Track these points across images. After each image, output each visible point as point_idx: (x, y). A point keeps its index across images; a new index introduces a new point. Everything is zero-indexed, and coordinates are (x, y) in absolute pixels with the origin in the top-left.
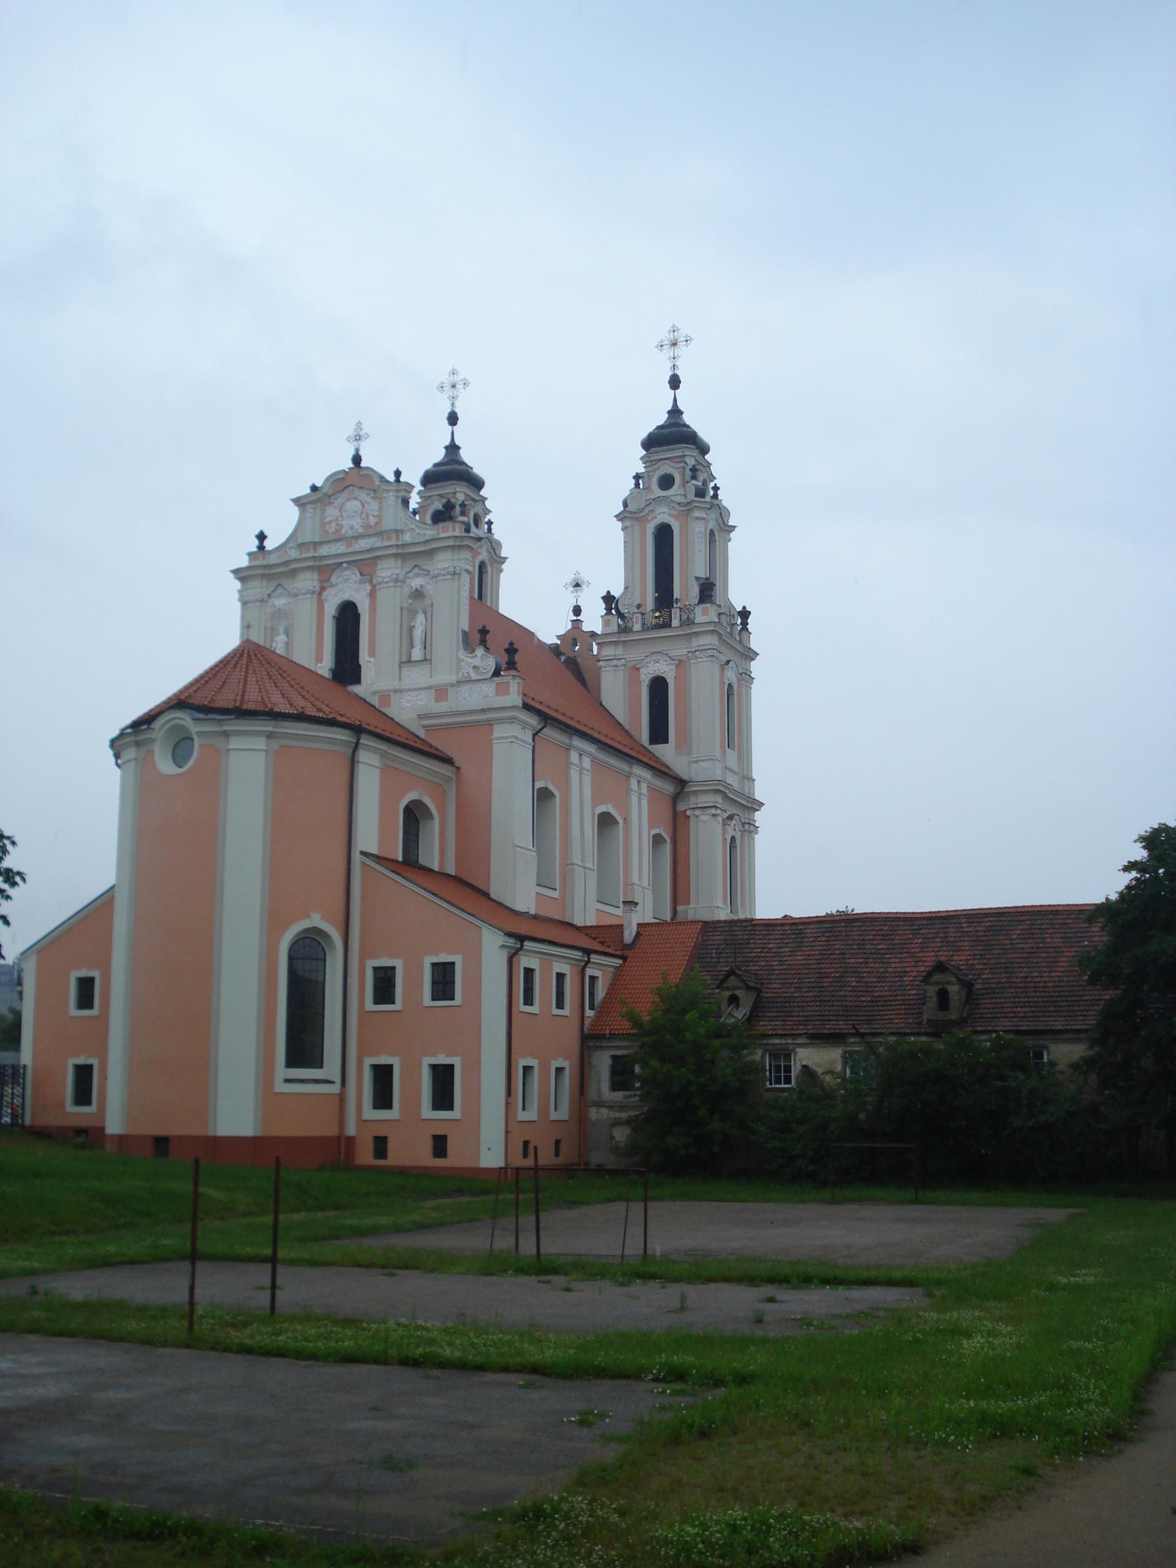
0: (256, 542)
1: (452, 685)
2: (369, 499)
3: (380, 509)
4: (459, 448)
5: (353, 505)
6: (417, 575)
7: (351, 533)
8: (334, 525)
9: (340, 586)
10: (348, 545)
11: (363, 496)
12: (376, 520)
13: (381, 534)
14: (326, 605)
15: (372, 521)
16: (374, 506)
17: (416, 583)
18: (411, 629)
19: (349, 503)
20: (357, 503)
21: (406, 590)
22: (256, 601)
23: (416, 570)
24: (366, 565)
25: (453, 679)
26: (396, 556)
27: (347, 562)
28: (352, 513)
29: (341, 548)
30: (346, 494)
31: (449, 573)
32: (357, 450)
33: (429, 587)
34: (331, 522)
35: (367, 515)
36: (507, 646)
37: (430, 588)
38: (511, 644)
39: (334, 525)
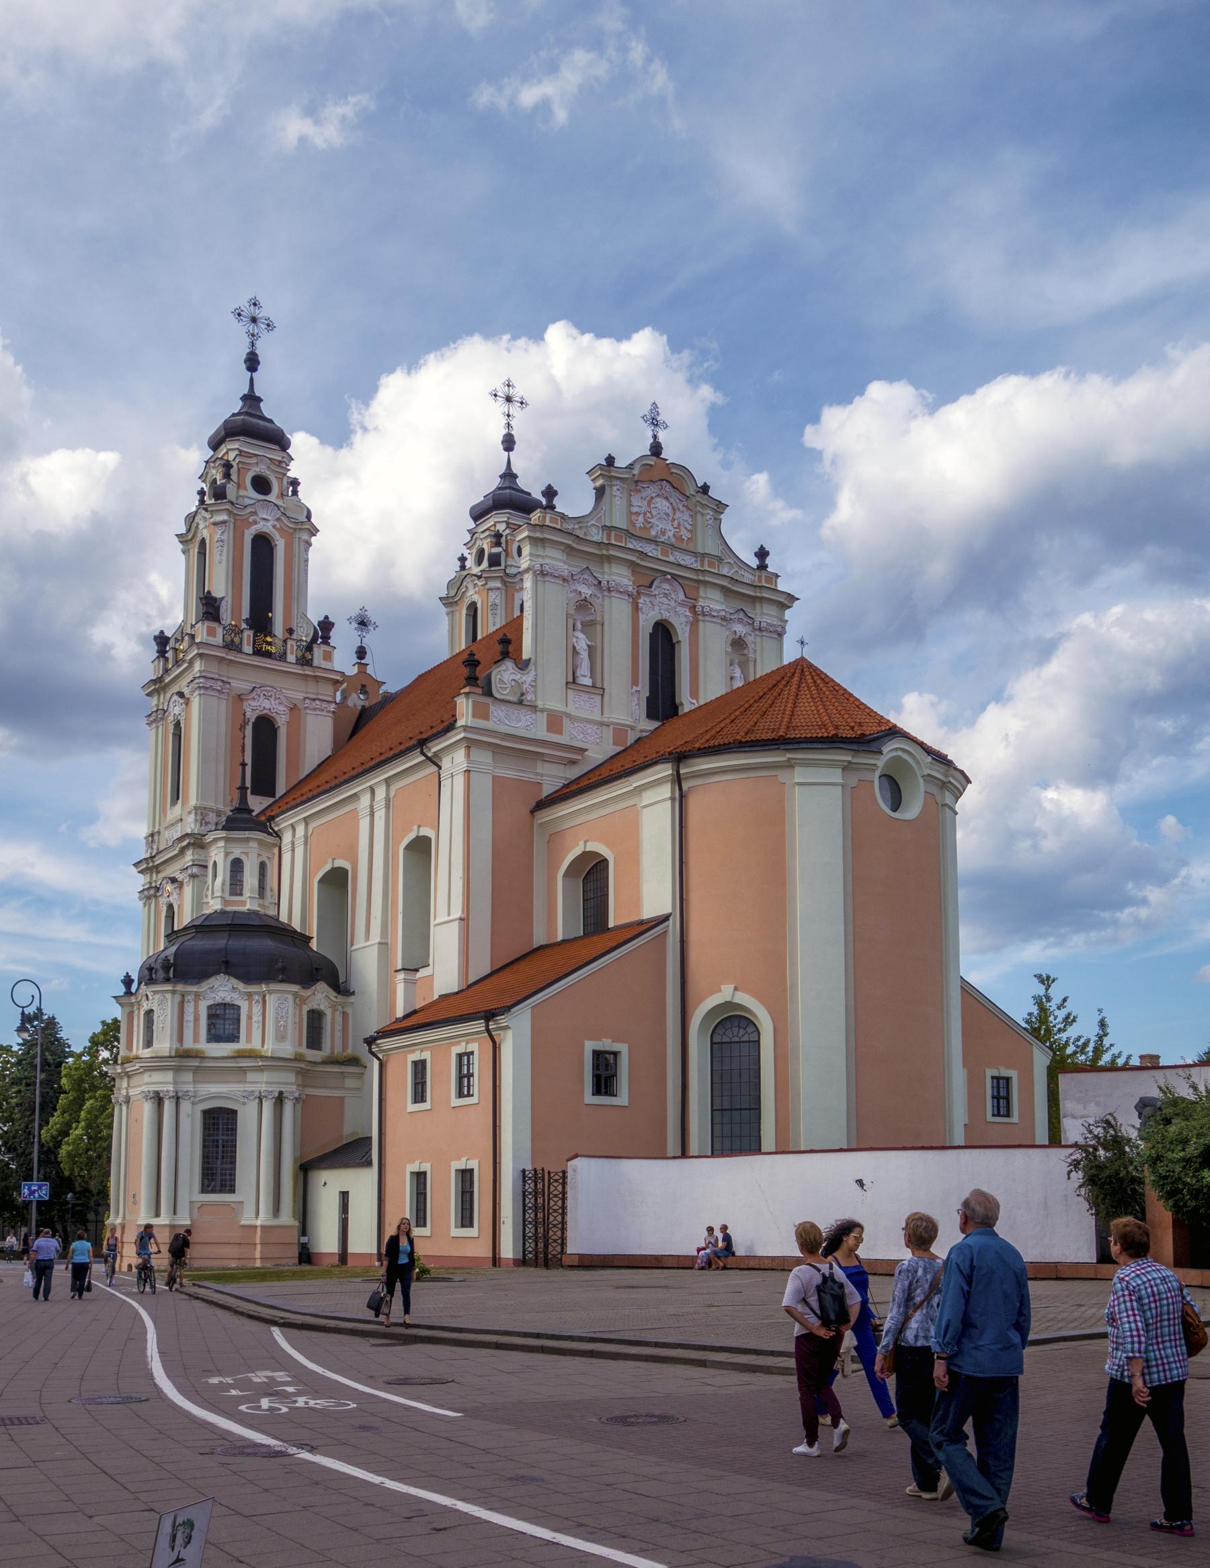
6: (740, 621)
9: (657, 601)
10: (665, 553)
13: (695, 554)
17: (740, 629)
24: (691, 585)
26: (723, 588)
28: (662, 515)
29: (688, 560)
37: (749, 640)
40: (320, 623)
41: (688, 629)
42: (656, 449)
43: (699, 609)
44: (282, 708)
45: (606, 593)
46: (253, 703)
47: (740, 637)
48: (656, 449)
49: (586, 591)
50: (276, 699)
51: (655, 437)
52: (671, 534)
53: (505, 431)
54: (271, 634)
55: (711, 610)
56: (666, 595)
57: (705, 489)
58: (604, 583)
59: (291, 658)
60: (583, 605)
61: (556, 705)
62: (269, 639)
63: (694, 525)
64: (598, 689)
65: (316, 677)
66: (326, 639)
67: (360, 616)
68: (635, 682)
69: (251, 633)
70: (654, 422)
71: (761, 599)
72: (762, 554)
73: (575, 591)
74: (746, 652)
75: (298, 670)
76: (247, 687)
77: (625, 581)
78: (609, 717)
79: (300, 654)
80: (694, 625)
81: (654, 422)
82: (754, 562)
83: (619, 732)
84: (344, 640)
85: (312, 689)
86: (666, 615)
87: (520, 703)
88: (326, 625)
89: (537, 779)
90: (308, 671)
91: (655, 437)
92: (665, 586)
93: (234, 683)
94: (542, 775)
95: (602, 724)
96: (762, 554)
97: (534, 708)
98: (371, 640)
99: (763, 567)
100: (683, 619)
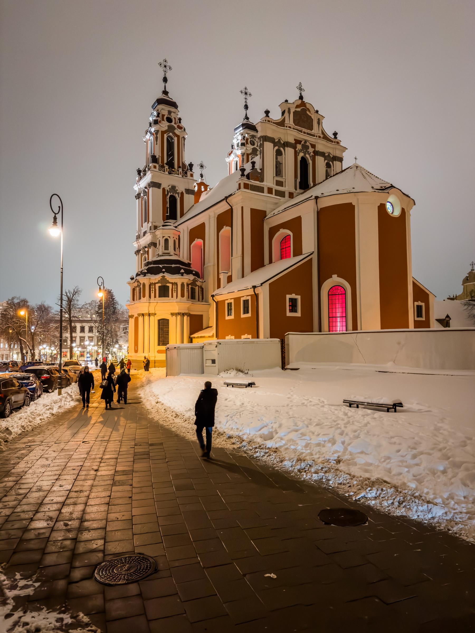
40: (189, 165)
42: (301, 98)
48: (301, 98)
51: (301, 94)
54: (175, 169)
57: (317, 112)
62: (173, 170)
66: (191, 170)
67: (201, 164)
69: (168, 168)
70: (301, 89)
72: (335, 134)
81: (301, 89)
82: (333, 137)
84: (196, 171)
88: (191, 165)
91: (301, 94)
96: (335, 134)
98: (204, 172)
99: (336, 138)
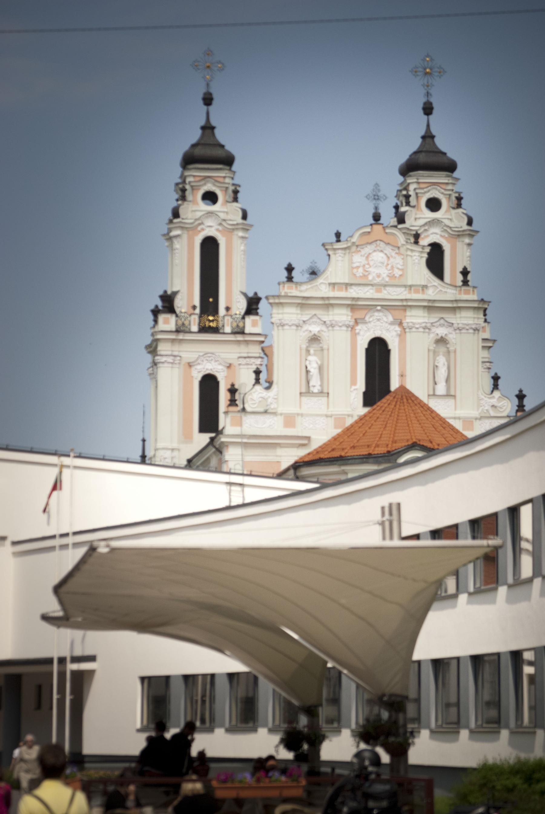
0: (285, 274)
1: (476, 419)
2: (393, 254)
3: (405, 264)
4: (213, 128)
5: (378, 257)
6: (442, 325)
7: (378, 280)
8: (361, 270)
11: (388, 250)
12: (400, 273)
14: (359, 338)
15: (397, 273)
16: (398, 261)
18: (436, 367)
19: (375, 254)
20: (381, 255)
21: (432, 336)
22: (293, 325)
23: (442, 321)
25: (475, 413)
27: (382, 306)
30: (373, 247)
31: (471, 328)
32: (376, 208)
33: (451, 336)
34: (358, 267)
35: (392, 267)
36: (517, 393)
37: (452, 337)
38: (521, 391)
39: (361, 270)
41: (397, 340)
43: (405, 325)
44: (220, 367)
45: (330, 328)
46: (199, 367)
47: (442, 337)
49: (315, 329)
50: (216, 361)
52: (385, 275)
53: (424, 100)
55: (414, 323)
56: (378, 320)
58: (328, 322)
59: (228, 329)
60: (315, 339)
61: (292, 409)
63: (405, 264)
64: (324, 393)
65: (246, 341)
68: (353, 382)
71: (459, 308)
73: (306, 330)
74: (448, 346)
75: (232, 338)
76: (196, 355)
77: (344, 318)
78: (333, 410)
79: (235, 324)
80: (402, 336)
83: (339, 420)
85: (244, 350)
86: (378, 334)
87: (266, 412)
89: (278, 459)
90: (240, 338)
92: (376, 314)
93: (183, 355)
94: (280, 456)
95: (327, 416)
97: (275, 414)
100: (394, 334)
